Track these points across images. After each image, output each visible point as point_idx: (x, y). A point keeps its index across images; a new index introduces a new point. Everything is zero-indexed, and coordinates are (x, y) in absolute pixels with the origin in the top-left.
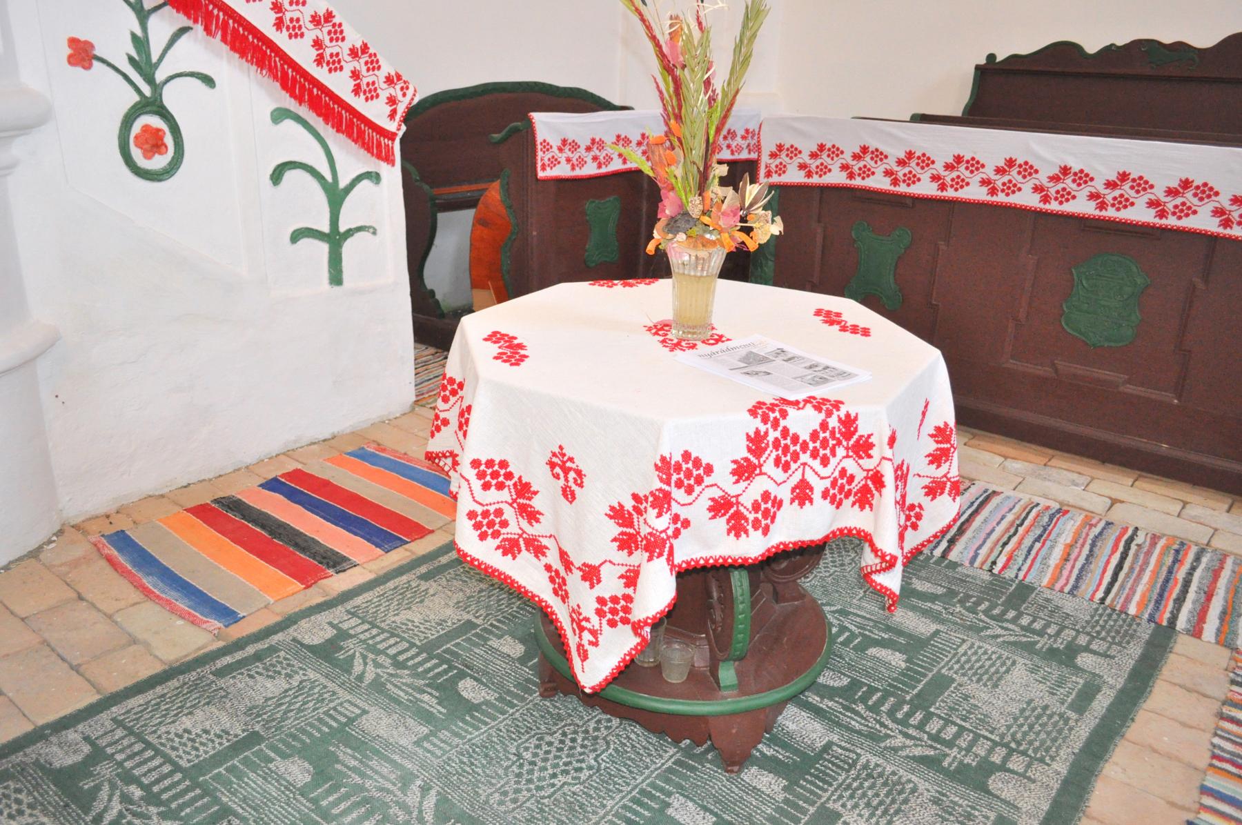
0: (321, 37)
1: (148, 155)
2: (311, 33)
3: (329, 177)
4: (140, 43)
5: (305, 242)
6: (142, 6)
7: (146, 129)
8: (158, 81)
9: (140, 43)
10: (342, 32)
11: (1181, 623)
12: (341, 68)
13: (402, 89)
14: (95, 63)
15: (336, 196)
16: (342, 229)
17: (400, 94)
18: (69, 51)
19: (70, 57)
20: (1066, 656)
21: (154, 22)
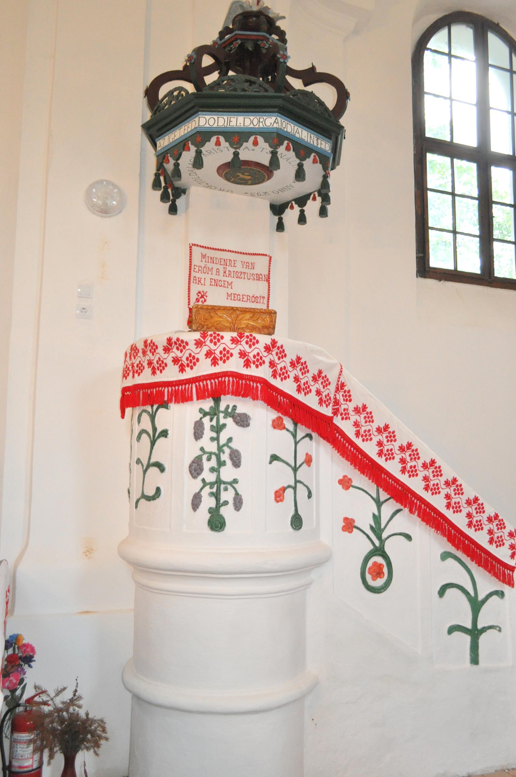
0: (471, 511)
1: (374, 579)
2: (466, 510)
3: (472, 593)
5: (457, 634)
6: (379, 500)
7: (375, 563)
8: (383, 538)
9: (377, 519)
10: (483, 508)
12: (482, 529)
14: (355, 530)
15: (476, 606)
16: (479, 627)
18: (343, 524)
19: (343, 527)
21: (384, 507)
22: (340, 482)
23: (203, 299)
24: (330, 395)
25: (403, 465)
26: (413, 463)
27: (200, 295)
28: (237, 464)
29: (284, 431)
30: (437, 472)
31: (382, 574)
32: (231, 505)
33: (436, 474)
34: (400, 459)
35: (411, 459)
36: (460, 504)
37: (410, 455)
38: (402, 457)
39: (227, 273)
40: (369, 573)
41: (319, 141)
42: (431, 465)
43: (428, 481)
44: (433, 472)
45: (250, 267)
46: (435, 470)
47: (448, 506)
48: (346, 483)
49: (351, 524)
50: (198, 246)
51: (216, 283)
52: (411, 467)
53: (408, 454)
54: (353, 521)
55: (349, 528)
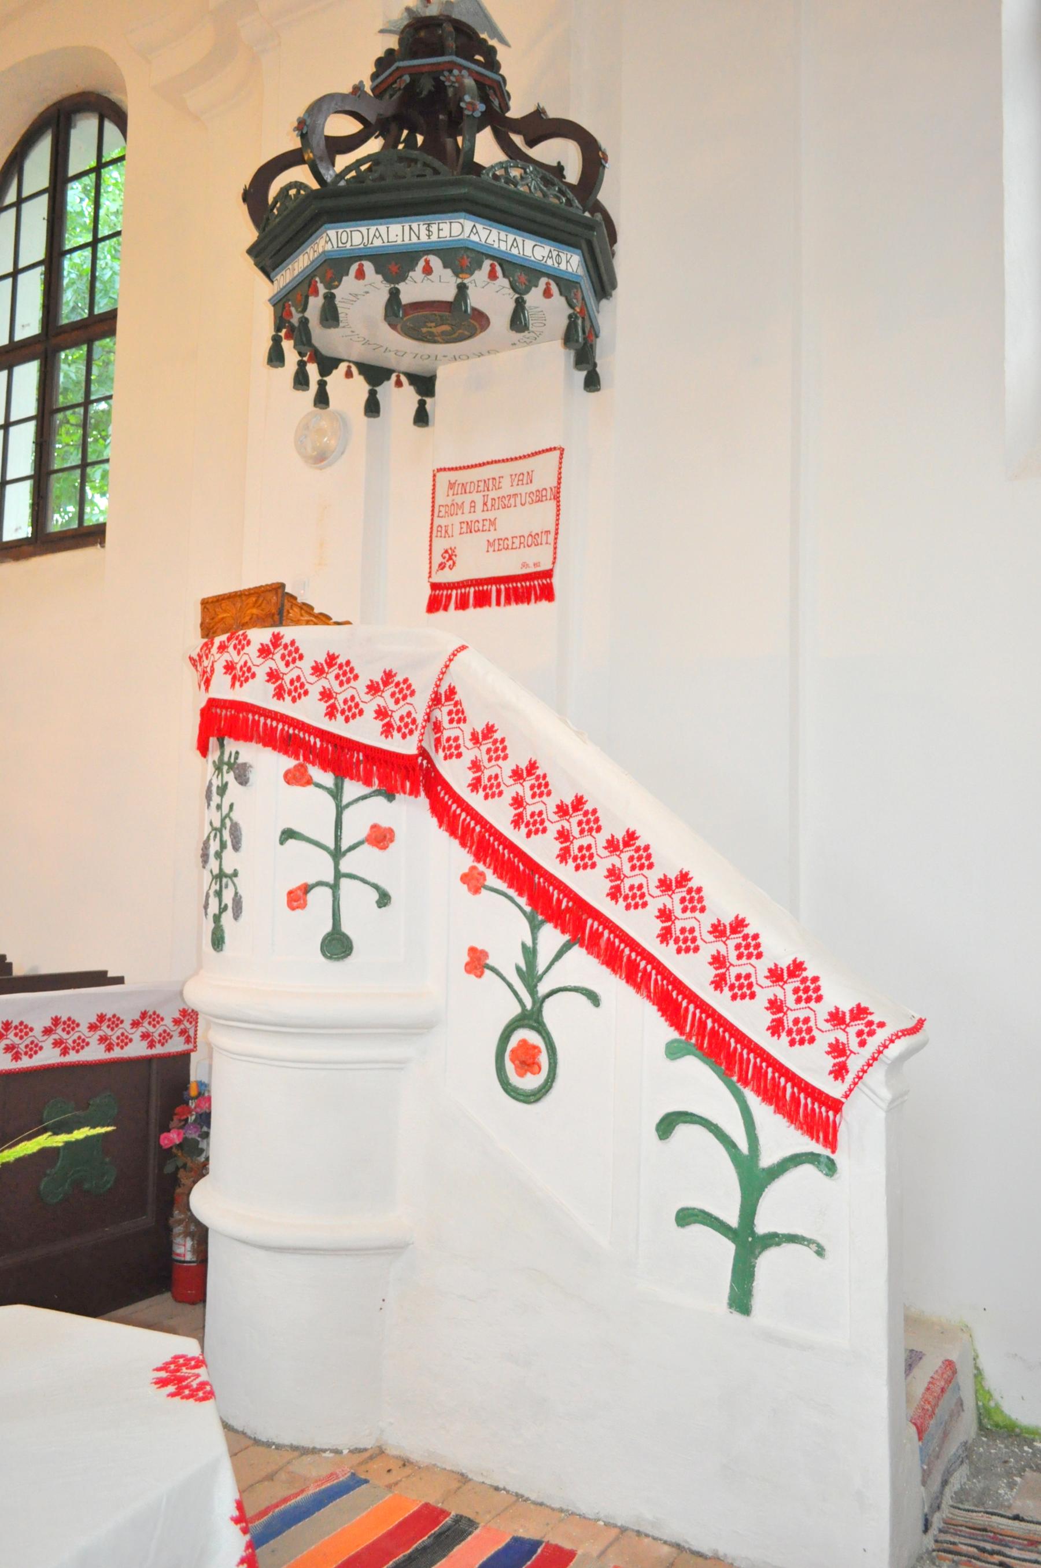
3: (743, 1146)
4: (530, 953)
5: (699, 1231)
7: (524, 1043)
9: (530, 953)
12: (753, 996)
13: (860, 1033)
14: (487, 972)
15: (755, 1179)
16: (762, 1226)
17: (853, 1043)
22: (465, 878)
23: (451, 562)
24: (414, 715)
25: (564, 845)
26: (585, 841)
27: (447, 556)
28: (236, 847)
29: (311, 788)
30: (640, 858)
31: (536, 1067)
32: (229, 912)
33: (638, 864)
34: (558, 832)
35: (582, 832)
36: (696, 934)
37: (580, 823)
38: (563, 827)
39: (489, 504)
40: (513, 1061)
41: (434, 228)
42: (627, 844)
43: (618, 878)
44: (631, 859)
45: (525, 482)
46: (636, 855)
47: (665, 936)
48: (473, 882)
49: (479, 959)
50: (445, 469)
51: (470, 528)
52: (581, 849)
53: (574, 821)
54: (484, 954)
55: (476, 968)
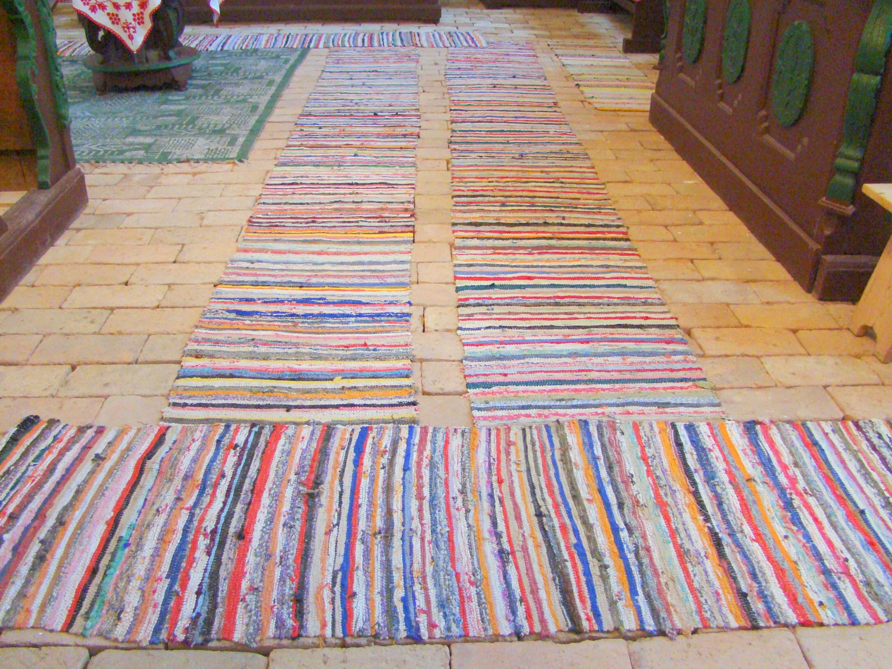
11: (312, 46)
20: (278, 57)
